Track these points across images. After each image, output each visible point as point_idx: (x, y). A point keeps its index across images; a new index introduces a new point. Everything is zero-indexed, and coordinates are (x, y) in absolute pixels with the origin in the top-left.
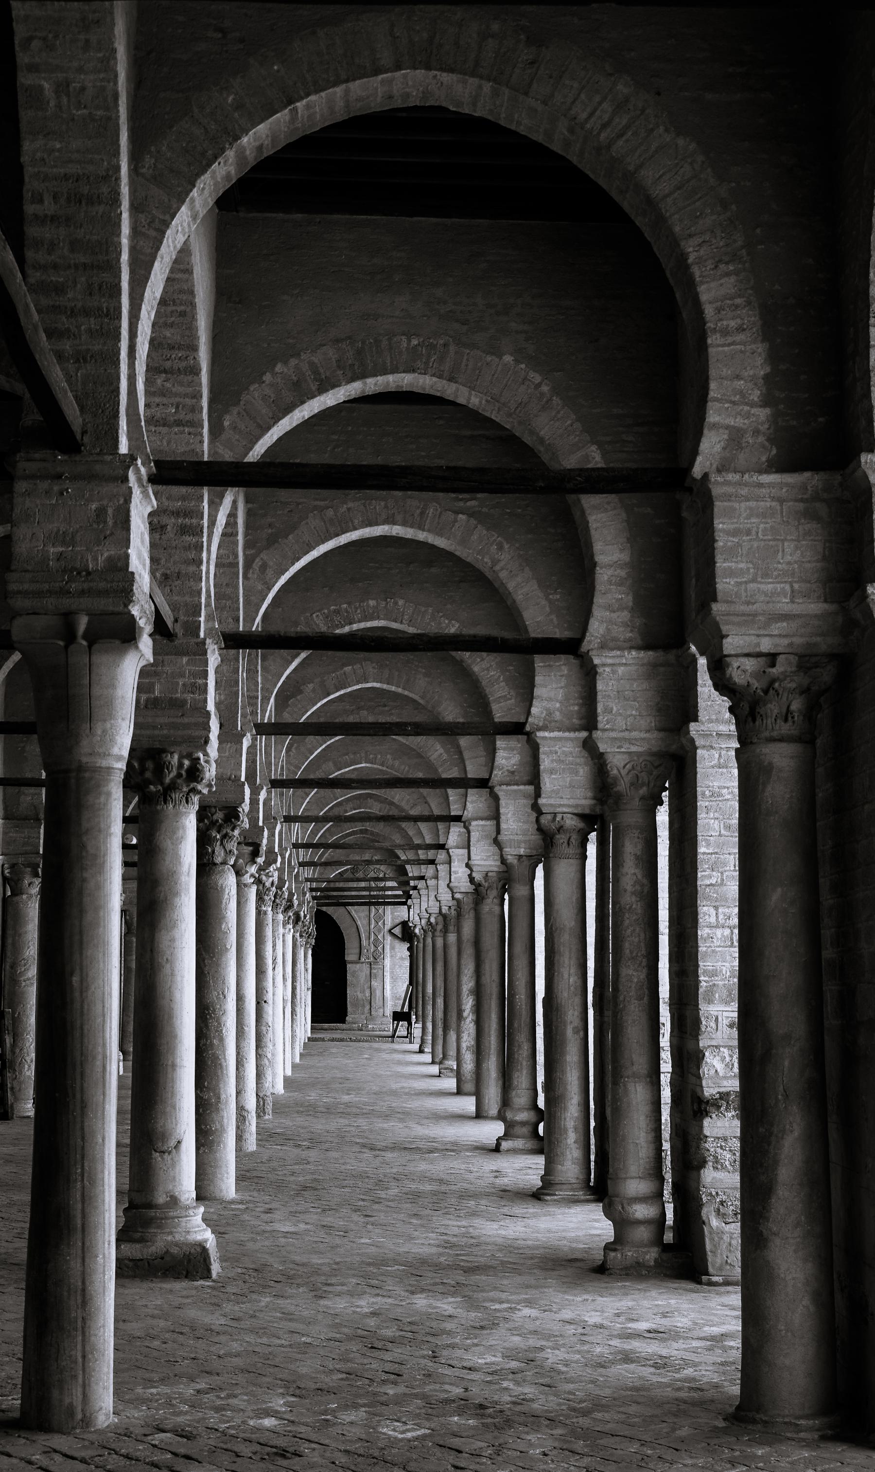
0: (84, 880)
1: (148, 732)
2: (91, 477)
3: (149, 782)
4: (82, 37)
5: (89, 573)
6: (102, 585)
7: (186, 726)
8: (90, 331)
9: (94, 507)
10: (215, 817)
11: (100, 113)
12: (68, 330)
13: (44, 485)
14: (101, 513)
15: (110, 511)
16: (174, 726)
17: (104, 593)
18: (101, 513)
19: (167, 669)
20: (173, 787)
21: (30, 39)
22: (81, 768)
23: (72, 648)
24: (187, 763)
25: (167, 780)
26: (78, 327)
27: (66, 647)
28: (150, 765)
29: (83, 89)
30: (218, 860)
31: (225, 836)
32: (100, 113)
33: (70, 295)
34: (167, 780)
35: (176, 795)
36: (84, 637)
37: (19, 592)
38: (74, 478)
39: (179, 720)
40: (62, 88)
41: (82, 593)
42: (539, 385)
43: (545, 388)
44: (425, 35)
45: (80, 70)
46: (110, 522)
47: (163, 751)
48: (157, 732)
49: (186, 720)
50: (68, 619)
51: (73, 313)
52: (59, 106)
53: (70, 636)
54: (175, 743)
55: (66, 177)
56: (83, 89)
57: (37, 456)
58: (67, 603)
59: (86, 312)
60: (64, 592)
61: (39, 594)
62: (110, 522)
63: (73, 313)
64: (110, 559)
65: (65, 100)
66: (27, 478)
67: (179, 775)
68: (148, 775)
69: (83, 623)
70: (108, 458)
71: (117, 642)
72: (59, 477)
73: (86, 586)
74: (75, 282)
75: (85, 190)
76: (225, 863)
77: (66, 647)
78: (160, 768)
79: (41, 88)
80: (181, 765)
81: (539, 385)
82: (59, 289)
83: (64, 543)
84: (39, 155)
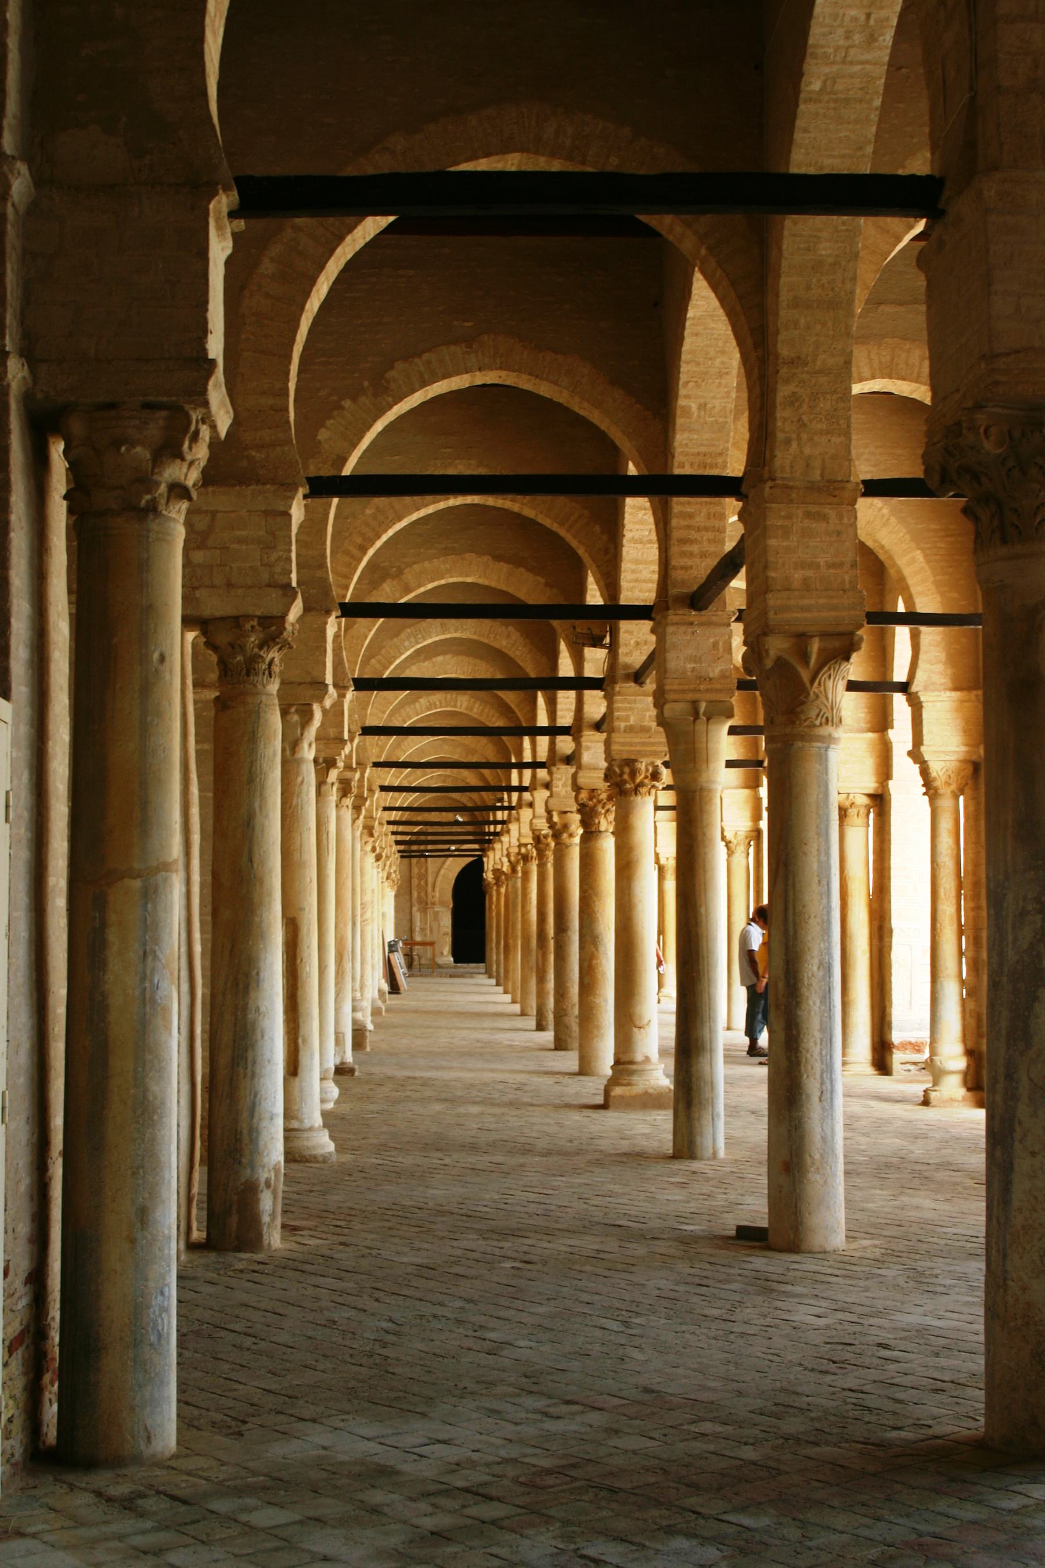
0: (705, 854)
1: (627, 748)
2: (709, 624)
3: (626, 782)
4: (717, 381)
5: (711, 679)
6: (718, 686)
7: (653, 744)
8: (709, 541)
9: (712, 640)
10: (601, 797)
11: (721, 420)
12: (696, 539)
13: (682, 629)
14: (715, 645)
15: (721, 643)
16: (644, 744)
17: (720, 691)
18: (715, 645)
19: (637, 705)
20: (641, 784)
21: (687, 383)
22: (702, 789)
23: (698, 721)
24: (651, 769)
25: (638, 781)
26: (702, 537)
27: (695, 720)
28: (627, 770)
29: (714, 407)
30: (602, 828)
31: (608, 811)
32: (721, 420)
33: (697, 519)
34: (638, 781)
35: (643, 790)
36: (704, 714)
37: (671, 690)
38: (701, 624)
39: (647, 740)
40: (702, 407)
41: (707, 691)
42: (880, 509)
43: (885, 511)
44: (888, 358)
45: (714, 397)
46: (721, 650)
47: (635, 761)
48: (633, 748)
49: (652, 740)
50: (695, 704)
51: (699, 529)
52: (699, 416)
53: (696, 715)
54: (645, 756)
55: (699, 454)
56: (714, 407)
57: (680, 612)
58: (697, 696)
59: (706, 529)
60: (696, 690)
61: (683, 691)
62: (721, 650)
63: (699, 529)
64: (721, 671)
65: (703, 413)
66: (673, 624)
67: (646, 777)
68: (626, 777)
69: (703, 706)
70: (720, 613)
71: (723, 718)
72: (692, 624)
73: (709, 686)
74: (700, 512)
75: (709, 461)
76: (606, 831)
77: (695, 720)
78: (633, 774)
79: (690, 408)
80: (647, 770)
81: (880, 509)
82: (691, 516)
83: (695, 662)
84: (684, 442)
